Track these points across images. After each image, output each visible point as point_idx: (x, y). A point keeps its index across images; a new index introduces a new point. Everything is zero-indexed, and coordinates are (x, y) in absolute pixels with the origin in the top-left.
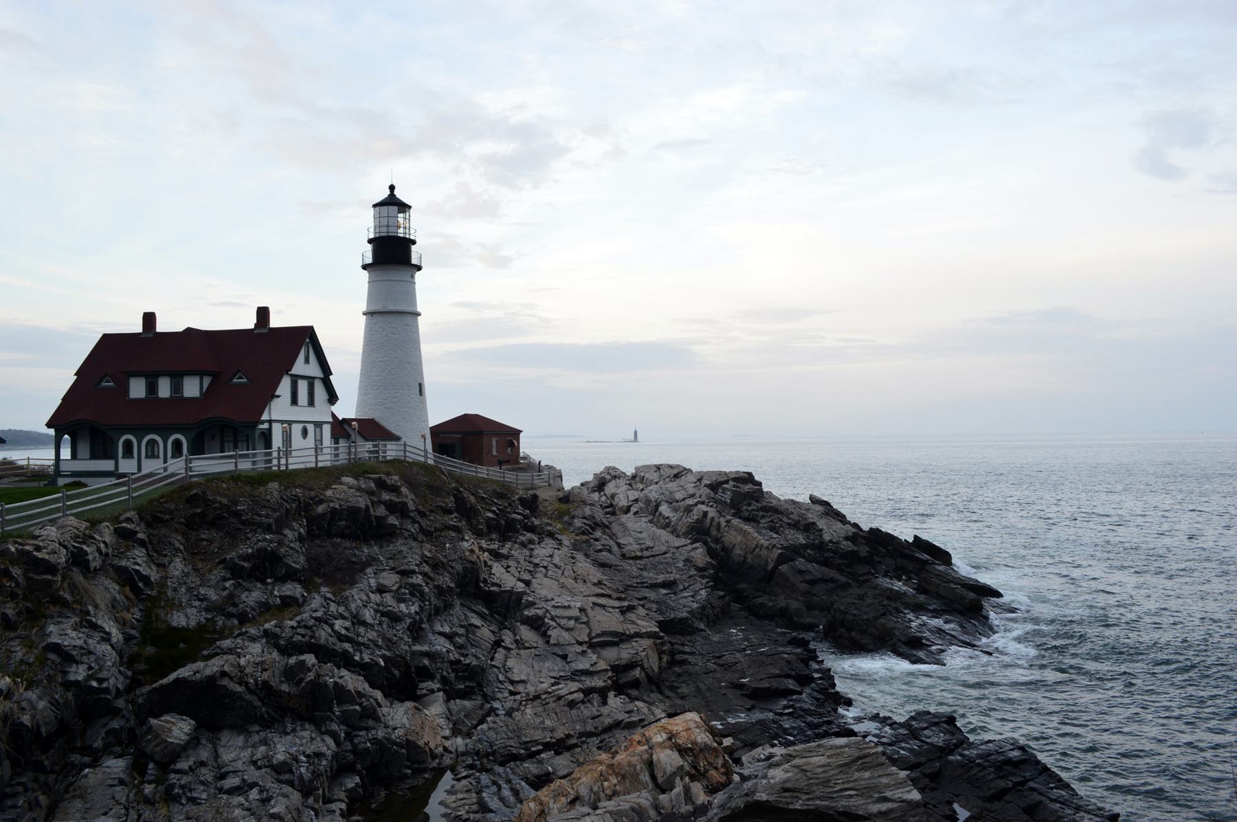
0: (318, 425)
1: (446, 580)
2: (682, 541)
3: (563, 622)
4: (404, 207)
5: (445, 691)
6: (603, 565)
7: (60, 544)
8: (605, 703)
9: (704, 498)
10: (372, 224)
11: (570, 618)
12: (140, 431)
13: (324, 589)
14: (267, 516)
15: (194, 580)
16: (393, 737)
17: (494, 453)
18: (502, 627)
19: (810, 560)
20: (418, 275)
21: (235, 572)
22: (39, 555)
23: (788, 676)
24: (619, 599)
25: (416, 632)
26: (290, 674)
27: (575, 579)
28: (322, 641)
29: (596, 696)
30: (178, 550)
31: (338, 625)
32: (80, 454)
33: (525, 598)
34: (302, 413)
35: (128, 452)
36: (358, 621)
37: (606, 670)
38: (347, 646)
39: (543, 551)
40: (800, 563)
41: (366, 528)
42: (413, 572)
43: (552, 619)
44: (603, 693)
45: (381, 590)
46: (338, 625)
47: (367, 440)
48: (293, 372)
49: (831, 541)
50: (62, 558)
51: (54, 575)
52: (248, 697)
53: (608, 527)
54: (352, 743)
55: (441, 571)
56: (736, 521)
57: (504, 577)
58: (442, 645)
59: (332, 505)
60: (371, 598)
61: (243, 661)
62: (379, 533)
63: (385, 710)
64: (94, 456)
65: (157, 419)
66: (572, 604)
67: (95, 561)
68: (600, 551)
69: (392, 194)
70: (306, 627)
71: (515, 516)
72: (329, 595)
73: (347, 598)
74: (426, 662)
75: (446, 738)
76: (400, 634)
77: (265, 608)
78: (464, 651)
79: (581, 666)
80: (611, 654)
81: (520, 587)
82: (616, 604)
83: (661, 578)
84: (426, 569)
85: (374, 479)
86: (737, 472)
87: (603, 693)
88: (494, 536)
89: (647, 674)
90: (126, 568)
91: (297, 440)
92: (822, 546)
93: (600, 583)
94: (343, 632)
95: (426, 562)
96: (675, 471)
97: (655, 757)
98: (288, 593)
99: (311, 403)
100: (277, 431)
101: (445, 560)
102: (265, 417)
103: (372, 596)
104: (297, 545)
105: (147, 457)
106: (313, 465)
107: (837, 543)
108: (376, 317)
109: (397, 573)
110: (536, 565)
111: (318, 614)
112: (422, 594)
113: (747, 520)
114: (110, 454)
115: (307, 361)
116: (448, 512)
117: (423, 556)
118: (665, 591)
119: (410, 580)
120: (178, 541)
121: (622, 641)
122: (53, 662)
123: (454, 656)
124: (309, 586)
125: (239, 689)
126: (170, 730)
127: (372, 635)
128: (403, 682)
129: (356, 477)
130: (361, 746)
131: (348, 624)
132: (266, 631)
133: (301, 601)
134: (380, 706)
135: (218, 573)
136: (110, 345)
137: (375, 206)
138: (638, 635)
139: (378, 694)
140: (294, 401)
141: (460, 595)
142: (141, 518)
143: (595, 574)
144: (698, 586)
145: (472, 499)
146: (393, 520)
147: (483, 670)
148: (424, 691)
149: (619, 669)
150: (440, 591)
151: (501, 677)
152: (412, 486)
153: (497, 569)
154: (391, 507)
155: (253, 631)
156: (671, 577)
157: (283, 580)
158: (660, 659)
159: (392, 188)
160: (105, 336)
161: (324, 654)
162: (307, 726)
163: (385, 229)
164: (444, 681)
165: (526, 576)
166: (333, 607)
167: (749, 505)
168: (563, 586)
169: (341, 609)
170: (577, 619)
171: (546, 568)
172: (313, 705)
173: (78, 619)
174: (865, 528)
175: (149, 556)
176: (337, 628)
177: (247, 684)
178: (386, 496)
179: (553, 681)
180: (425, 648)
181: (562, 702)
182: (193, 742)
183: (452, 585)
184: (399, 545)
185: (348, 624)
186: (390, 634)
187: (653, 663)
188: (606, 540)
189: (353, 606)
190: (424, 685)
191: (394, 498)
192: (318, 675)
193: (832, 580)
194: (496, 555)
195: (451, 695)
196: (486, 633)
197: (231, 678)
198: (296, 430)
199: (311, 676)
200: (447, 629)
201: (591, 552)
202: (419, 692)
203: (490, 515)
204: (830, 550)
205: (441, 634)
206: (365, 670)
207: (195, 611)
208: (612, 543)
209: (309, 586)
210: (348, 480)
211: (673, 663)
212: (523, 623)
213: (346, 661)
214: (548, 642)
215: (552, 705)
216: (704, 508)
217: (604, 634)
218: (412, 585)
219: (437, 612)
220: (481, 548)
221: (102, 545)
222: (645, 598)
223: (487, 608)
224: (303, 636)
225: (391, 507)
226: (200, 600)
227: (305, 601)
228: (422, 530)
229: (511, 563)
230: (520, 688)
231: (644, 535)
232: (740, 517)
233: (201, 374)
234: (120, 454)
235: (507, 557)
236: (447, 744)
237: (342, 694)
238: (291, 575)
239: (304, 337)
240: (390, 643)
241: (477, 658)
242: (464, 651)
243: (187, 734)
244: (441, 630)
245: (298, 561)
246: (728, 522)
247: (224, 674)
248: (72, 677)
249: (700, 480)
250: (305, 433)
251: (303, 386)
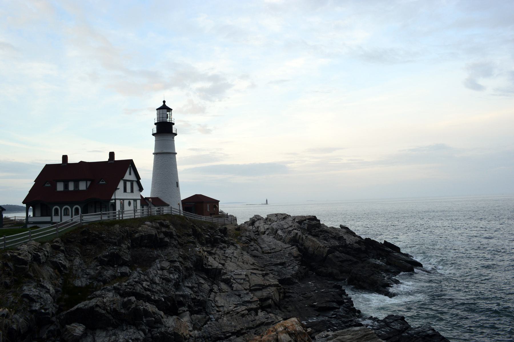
0: (135, 200)
1: (189, 264)
2: (287, 246)
3: (238, 281)
4: (169, 110)
5: (190, 311)
6: (254, 256)
7: (28, 252)
8: (257, 315)
9: (296, 227)
10: (156, 117)
11: (241, 279)
12: (61, 205)
13: (138, 269)
14: (114, 239)
15: (84, 266)
16: (168, 331)
17: (208, 210)
18: (213, 283)
19: (341, 252)
20: (175, 137)
21: (101, 262)
22: (20, 257)
23: (333, 301)
24: (262, 270)
25: (177, 286)
26: (125, 305)
27: (243, 263)
28: (138, 291)
29: (253, 312)
30: (77, 254)
31: (145, 284)
32: (36, 215)
33: (222, 271)
34: (129, 196)
35: (56, 213)
36: (153, 282)
37: (257, 301)
38: (148, 293)
39: (230, 251)
40: (337, 253)
41: (155, 243)
42: (176, 261)
43: (234, 279)
44: (256, 310)
45: (162, 269)
46: (145, 284)
47: (155, 206)
49: (349, 244)
50: (29, 258)
51: (26, 265)
52: (107, 315)
53: (256, 240)
54: (151, 334)
55: (187, 260)
56: (310, 237)
57: (213, 262)
58: (188, 292)
59: (141, 233)
60: (159, 272)
61: (105, 300)
62: (161, 245)
63: (165, 320)
64: (42, 215)
65: (69, 199)
66: (242, 273)
67: (43, 259)
68: (253, 250)
69: (164, 105)
70: (131, 285)
71: (217, 236)
72: (141, 272)
73: (148, 273)
74: (182, 299)
75: (191, 331)
76: (170, 287)
77: (114, 278)
78: (197, 294)
79: (246, 299)
80: (259, 294)
81: (220, 266)
82: (260, 272)
83: (279, 261)
84: (181, 259)
85: (158, 223)
86: (310, 216)
87: (256, 310)
88: (209, 245)
89: (274, 302)
90: (56, 262)
91: (126, 207)
92: (346, 246)
93: (253, 264)
94: (147, 287)
95: (181, 257)
96: (284, 216)
97: (279, 337)
98: (123, 271)
99: (132, 191)
100: (118, 203)
101: (189, 256)
102: (113, 197)
103: (159, 271)
104: (127, 251)
105: (64, 215)
106: (133, 217)
107: (352, 244)
108: (158, 156)
109: (169, 261)
110: (227, 257)
111: (136, 280)
112: (179, 270)
113: (314, 236)
114: (50, 215)
116: (189, 235)
117: (179, 254)
118: (281, 267)
119: (174, 265)
120: (77, 250)
121: (263, 288)
122: (26, 302)
123: (193, 296)
124: (132, 268)
125: (103, 312)
126: (75, 330)
127: (159, 288)
128: (172, 308)
129: (151, 222)
130: (155, 335)
131: (149, 283)
132: (114, 287)
133: (129, 274)
134: (163, 318)
135: (94, 263)
136: (49, 169)
137: (157, 109)
138: (270, 285)
139: (162, 313)
140: (125, 191)
141: (195, 271)
142: (62, 241)
143: (251, 260)
144: (295, 264)
145: (200, 230)
146: (167, 239)
147: (206, 302)
148: (181, 311)
149: (262, 300)
150: (187, 269)
151: (213, 305)
152: (174, 225)
153: (211, 259)
154: (166, 234)
155: (109, 287)
156: (283, 261)
157: (121, 265)
158: (280, 295)
159: (164, 102)
160: (47, 166)
161: (139, 296)
162: (132, 327)
163: (161, 119)
164: (189, 307)
165: (223, 262)
166: (142, 277)
167: (315, 230)
168: (238, 266)
169: (146, 277)
170: (244, 279)
171: (231, 258)
172: (134, 318)
173: (36, 284)
174: (363, 237)
175: (66, 257)
176: (144, 285)
177: (107, 310)
178: (164, 230)
179: (235, 306)
180: (181, 293)
181: (239, 315)
182: (85, 335)
183: (192, 266)
184: (170, 250)
185: (149, 283)
186: (166, 287)
187: (277, 297)
188: (256, 246)
189: (151, 276)
190: (180, 309)
191: (167, 230)
192: (137, 306)
193: (350, 260)
194: (210, 253)
195: (192, 313)
196: (206, 286)
197: (100, 307)
198: (126, 203)
199: (133, 306)
200: (190, 285)
201: (250, 251)
202: (179, 312)
203: (207, 236)
204: (349, 248)
205: (188, 287)
206: (156, 303)
207: (85, 279)
208: (258, 247)
209: (132, 268)
210: (148, 223)
211: (285, 297)
212: (222, 281)
213: (148, 299)
214: (232, 289)
215: (235, 316)
216: (296, 231)
217: (256, 285)
218: (175, 267)
219: (186, 277)
220: (203, 250)
221: (46, 252)
222: (273, 270)
223: (206, 275)
224: (130, 289)
225: (166, 234)
226: (86, 274)
227: (130, 275)
228: (178, 242)
229: (216, 256)
230: (221, 309)
231: (272, 243)
232: (311, 235)
233: (86, 180)
234: (53, 214)
235: (214, 254)
236: (191, 333)
237: (146, 313)
238: (125, 264)
239: (129, 164)
240: (166, 291)
241: (203, 297)
242: (197, 294)
243: (82, 332)
244: (187, 285)
245: (127, 258)
246: (306, 237)
247: (97, 306)
248: (34, 308)
249: (294, 220)
251: (128, 185)
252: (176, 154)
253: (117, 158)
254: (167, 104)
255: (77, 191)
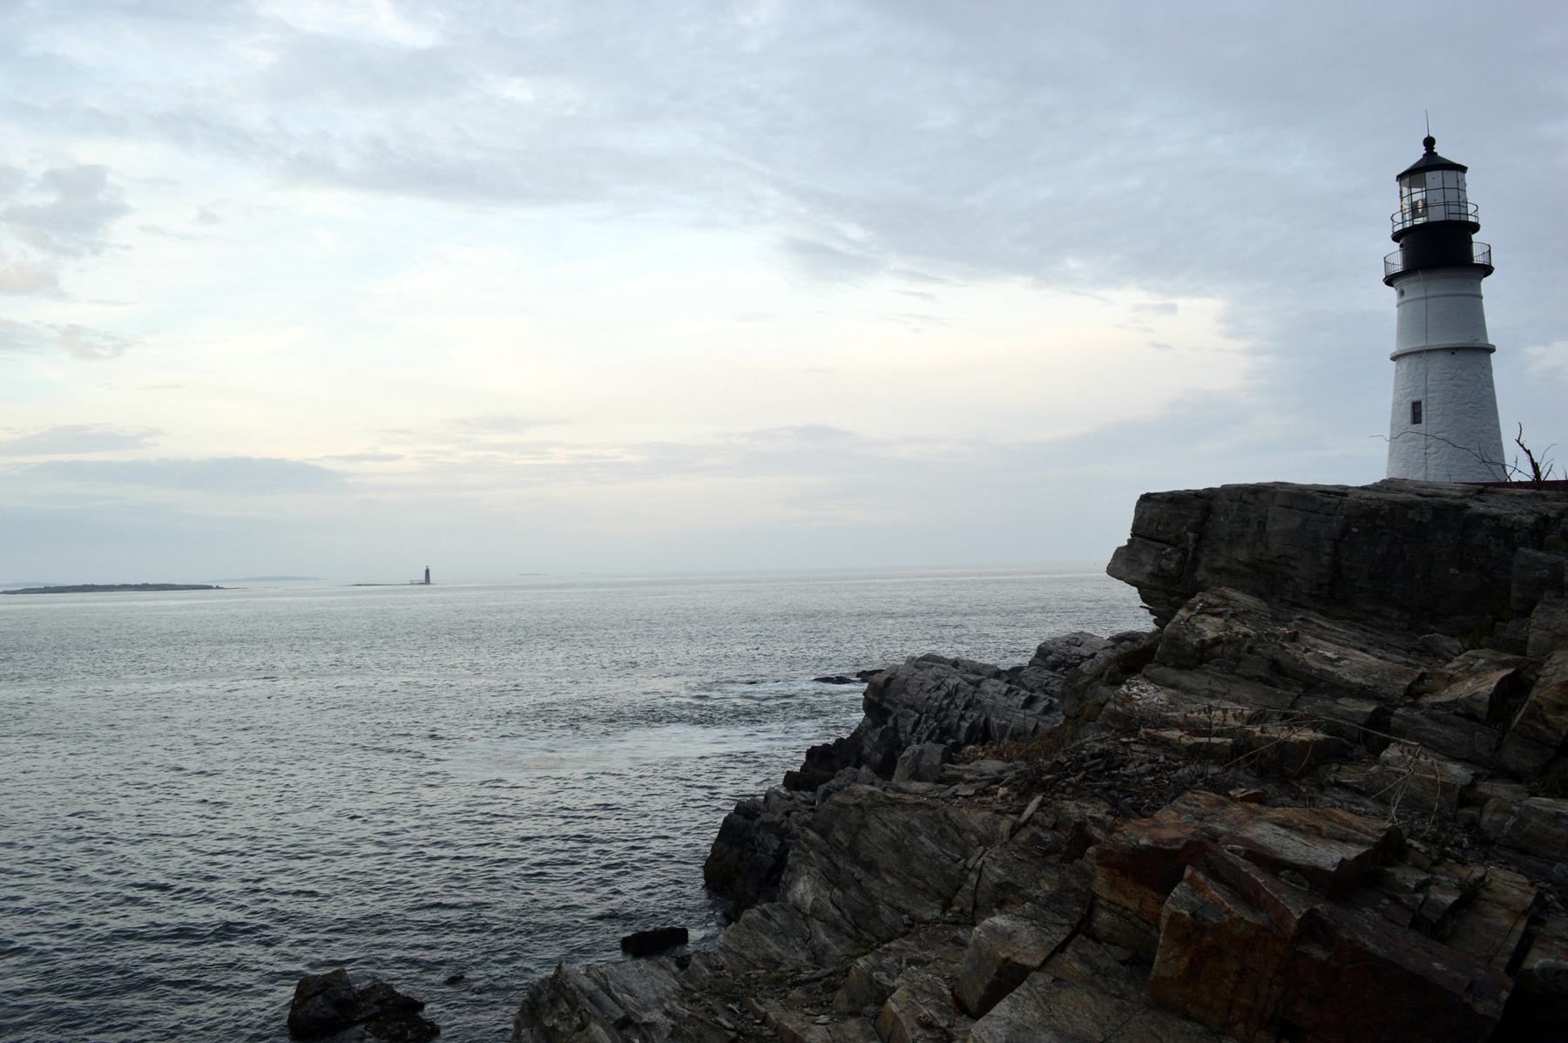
20: (1486, 284)
108: (1405, 362)
137: (1400, 177)
159: (1429, 142)
252: (1491, 350)
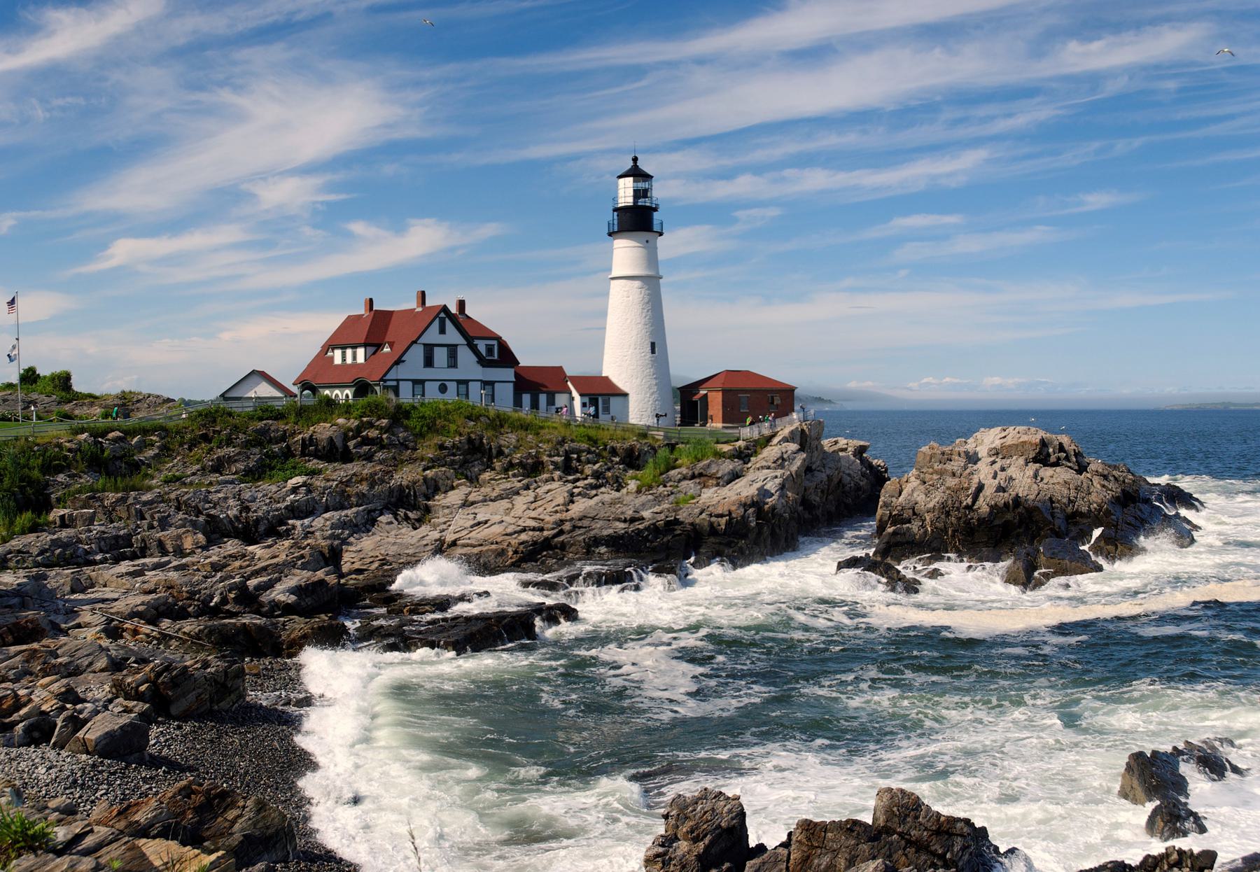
0: (465, 382)
48: (426, 339)
69: (635, 166)
102: (390, 376)
115: (442, 331)
140: (429, 362)
159: (635, 160)
225: (367, 441)
250: (443, 389)
253: (428, 304)
254: (644, 166)
255: (355, 365)
